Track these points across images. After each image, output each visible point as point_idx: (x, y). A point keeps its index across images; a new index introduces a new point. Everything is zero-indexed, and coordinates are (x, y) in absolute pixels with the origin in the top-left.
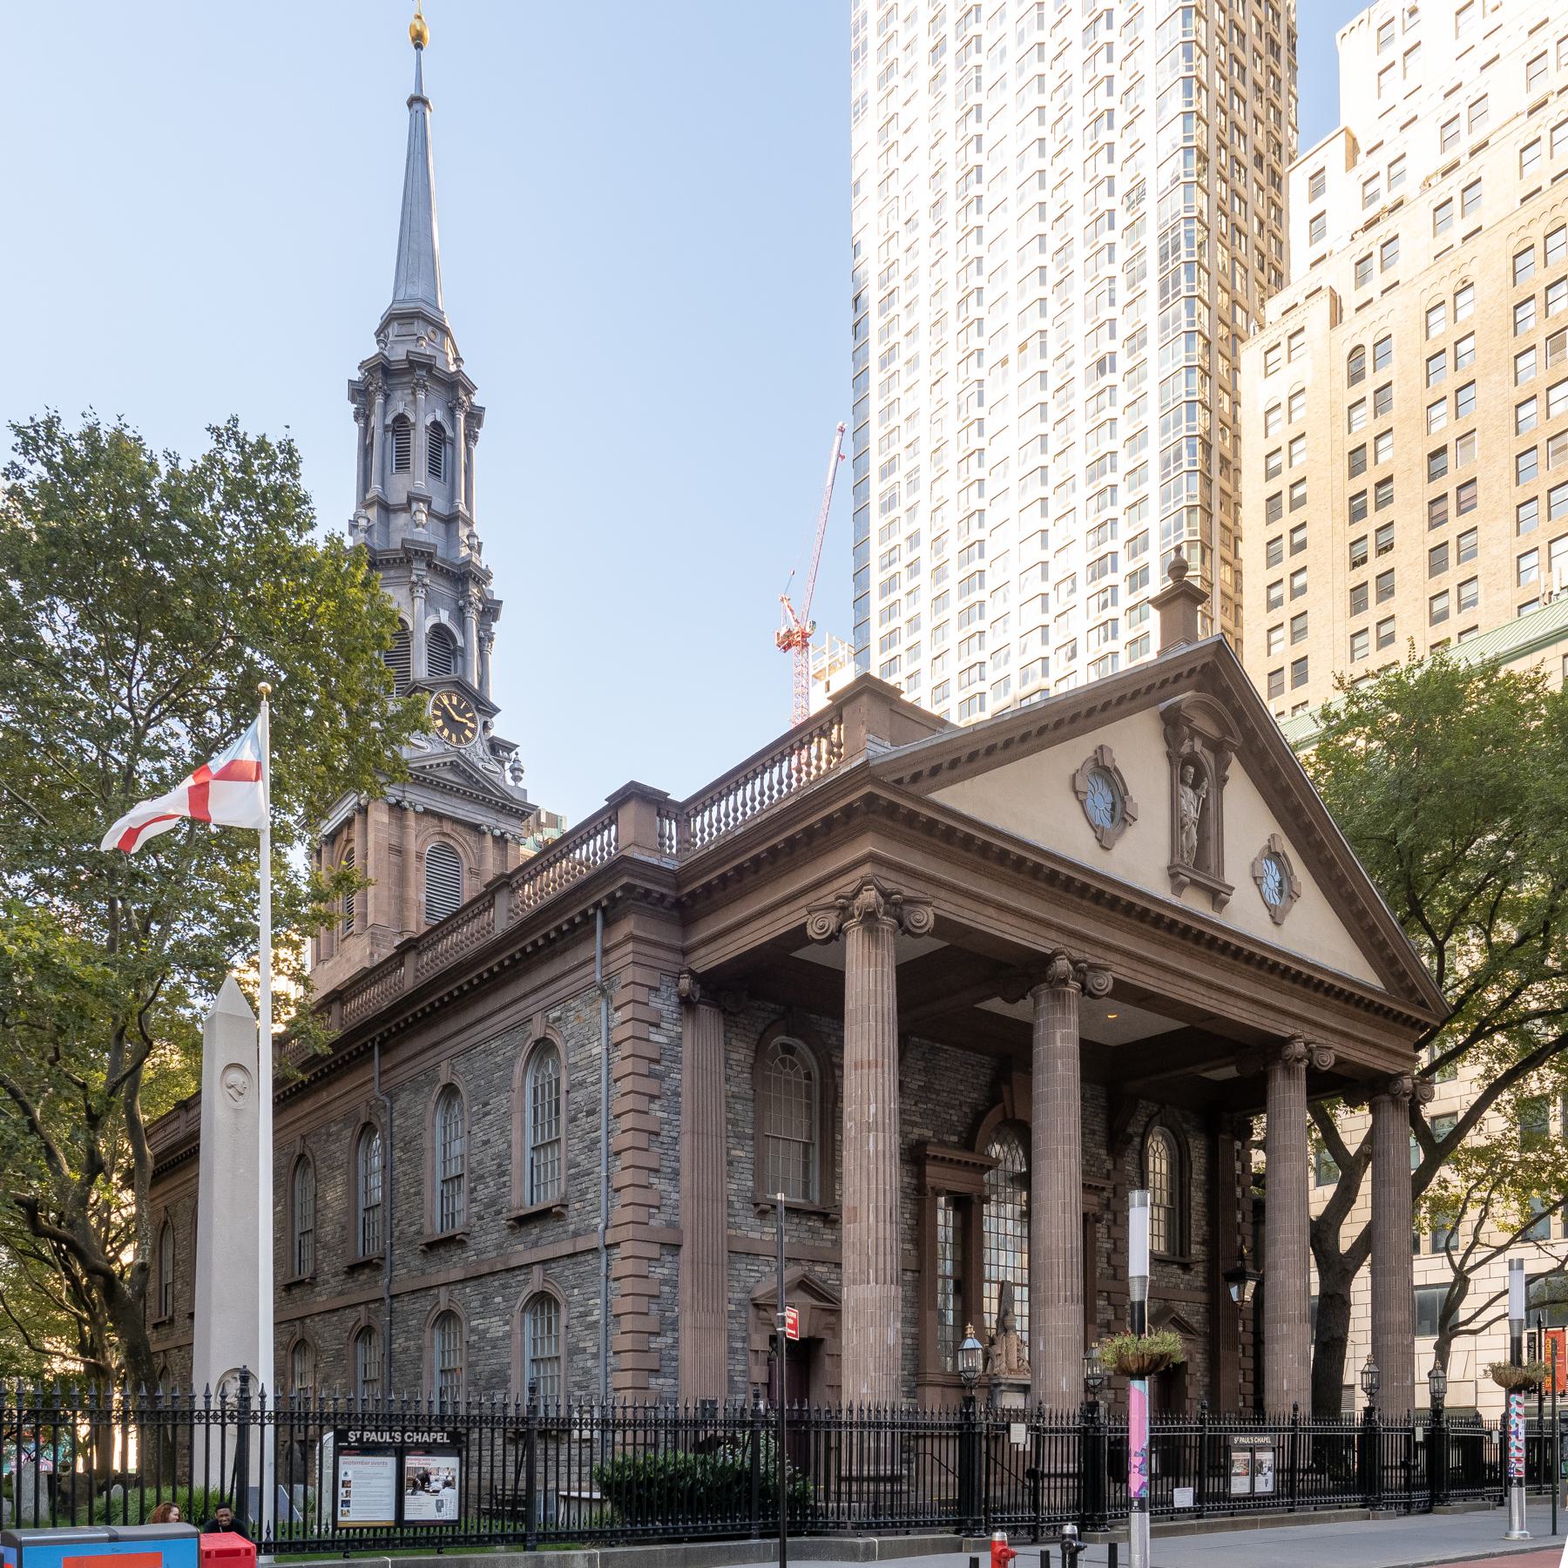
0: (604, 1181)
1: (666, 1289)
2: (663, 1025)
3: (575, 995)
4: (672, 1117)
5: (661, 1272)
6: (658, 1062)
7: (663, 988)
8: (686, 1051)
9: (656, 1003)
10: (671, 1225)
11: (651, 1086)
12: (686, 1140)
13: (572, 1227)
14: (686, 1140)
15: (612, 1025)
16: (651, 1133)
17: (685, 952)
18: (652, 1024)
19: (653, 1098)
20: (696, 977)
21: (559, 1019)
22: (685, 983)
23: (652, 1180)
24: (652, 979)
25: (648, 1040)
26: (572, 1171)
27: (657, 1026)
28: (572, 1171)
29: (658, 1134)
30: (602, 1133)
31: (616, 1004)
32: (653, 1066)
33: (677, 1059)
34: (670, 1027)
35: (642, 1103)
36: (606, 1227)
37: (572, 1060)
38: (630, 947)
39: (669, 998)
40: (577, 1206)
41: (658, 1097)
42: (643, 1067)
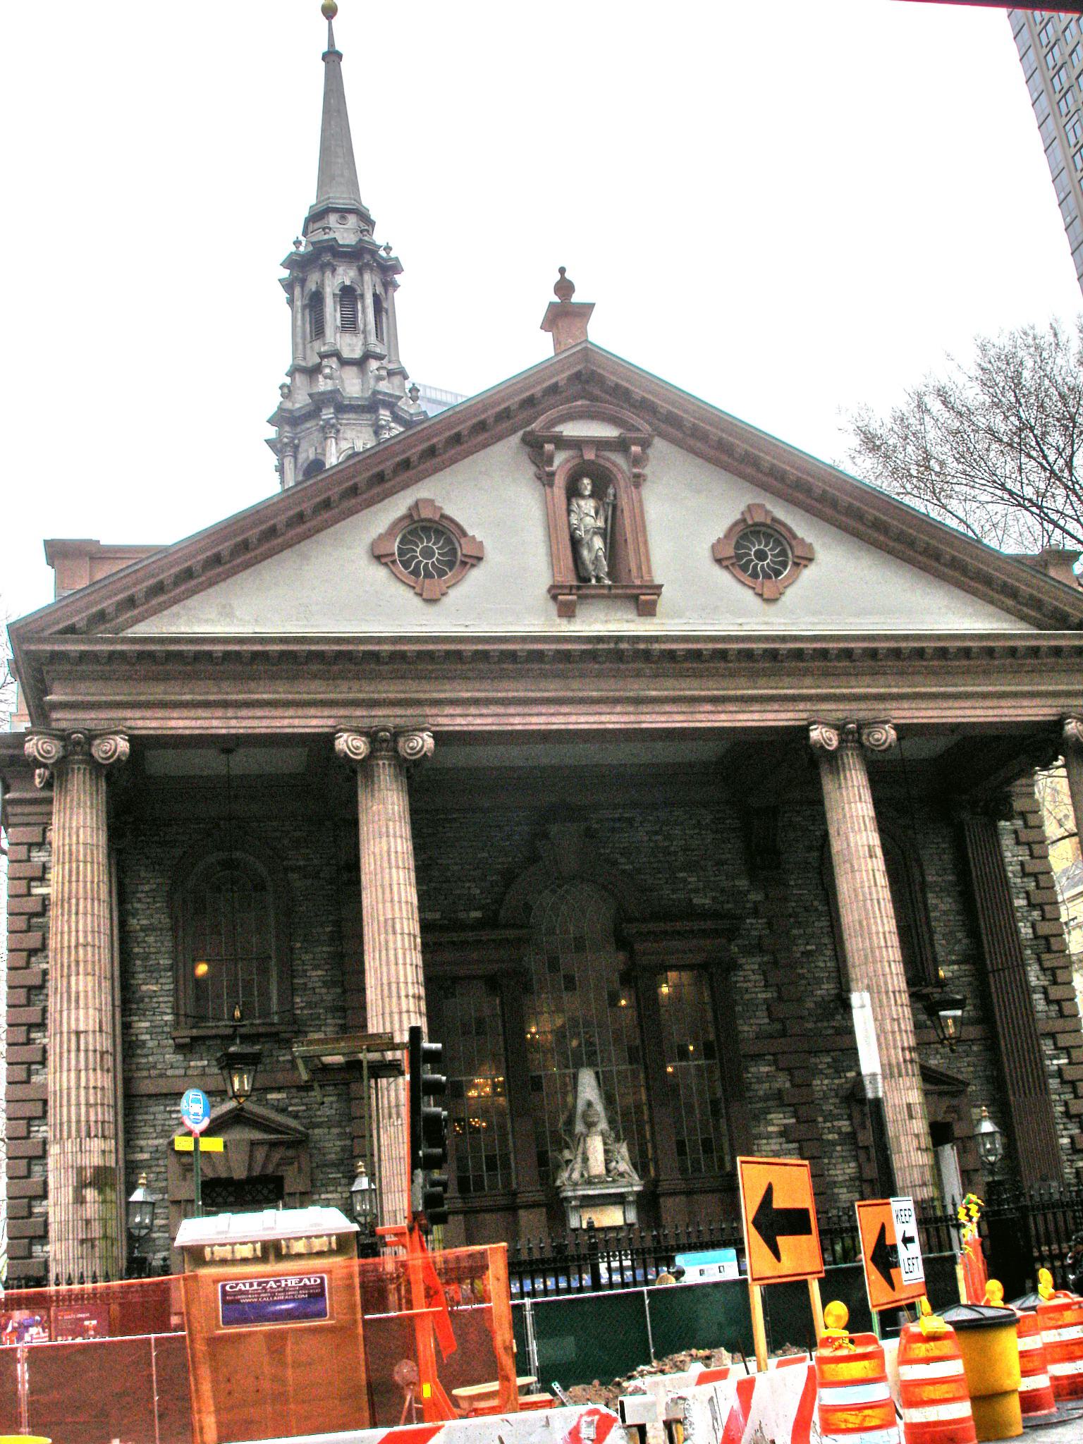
23: (33, 1035)
32: (35, 920)
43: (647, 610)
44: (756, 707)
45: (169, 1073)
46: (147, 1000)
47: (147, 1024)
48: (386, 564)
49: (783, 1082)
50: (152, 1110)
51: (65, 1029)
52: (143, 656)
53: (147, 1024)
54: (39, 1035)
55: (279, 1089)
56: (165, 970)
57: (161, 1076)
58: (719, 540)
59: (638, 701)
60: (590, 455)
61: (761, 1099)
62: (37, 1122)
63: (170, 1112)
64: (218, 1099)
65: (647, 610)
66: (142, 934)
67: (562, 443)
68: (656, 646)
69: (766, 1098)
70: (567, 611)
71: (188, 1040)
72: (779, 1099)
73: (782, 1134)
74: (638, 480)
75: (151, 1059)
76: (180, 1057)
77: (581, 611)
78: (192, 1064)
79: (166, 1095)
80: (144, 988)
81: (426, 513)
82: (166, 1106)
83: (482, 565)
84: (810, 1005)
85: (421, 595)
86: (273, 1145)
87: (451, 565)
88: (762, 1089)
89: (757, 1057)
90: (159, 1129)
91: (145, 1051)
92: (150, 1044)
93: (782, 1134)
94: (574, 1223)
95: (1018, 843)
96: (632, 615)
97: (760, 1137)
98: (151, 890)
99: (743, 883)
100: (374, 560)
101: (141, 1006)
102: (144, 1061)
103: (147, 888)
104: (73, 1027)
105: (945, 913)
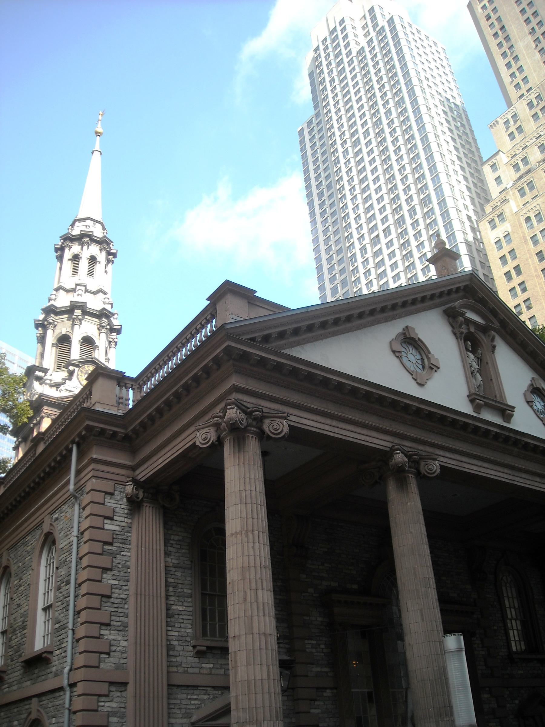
0: (70, 632)
1: (114, 719)
2: (115, 518)
3: (64, 503)
4: (122, 583)
5: (107, 706)
6: (111, 544)
7: (116, 493)
8: (133, 537)
9: (110, 503)
10: (119, 667)
11: (105, 561)
12: (132, 600)
13: (54, 669)
14: (132, 600)
15: (81, 520)
16: (103, 596)
17: (134, 468)
18: (106, 518)
19: (105, 570)
20: (137, 483)
21: (57, 519)
22: (129, 488)
23: (103, 632)
24: (108, 486)
25: (103, 529)
26: (57, 626)
27: (111, 519)
28: (57, 626)
29: (109, 597)
30: (72, 598)
31: (83, 505)
32: (106, 547)
33: (125, 542)
34: (122, 519)
35: (96, 574)
36: (71, 670)
37: (61, 546)
38: (92, 466)
39: (122, 499)
40: (58, 652)
41: (111, 570)
42: (98, 547)
45: (191, 670)
46: (176, 616)
47: (176, 634)
48: (398, 357)
50: (179, 696)
51: (256, 630)
52: (294, 372)
53: (176, 634)
54: (107, 632)
56: (188, 597)
57: (186, 672)
58: (525, 391)
62: (103, 699)
63: (190, 699)
64: (220, 692)
66: (174, 569)
70: (477, 409)
71: (205, 648)
75: (178, 659)
76: (197, 660)
78: (204, 665)
79: (188, 686)
80: (174, 607)
82: (188, 694)
83: (438, 371)
85: (416, 380)
90: (183, 711)
91: (175, 653)
92: (178, 648)
98: (179, 540)
100: (392, 353)
101: (173, 619)
102: (174, 660)
103: (177, 538)
104: (263, 630)
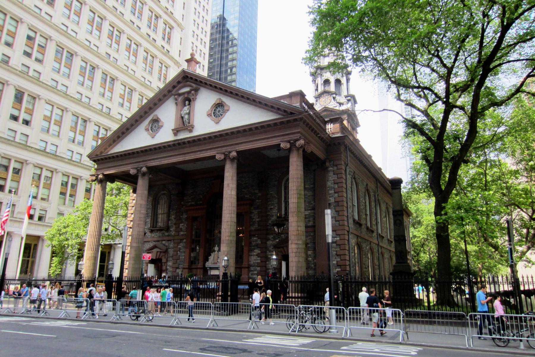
43: (191, 131)
44: (209, 151)
49: (259, 242)
55: (164, 241)
59: (184, 154)
60: (186, 96)
61: (254, 246)
65: (191, 131)
67: (180, 95)
68: (186, 140)
69: (254, 246)
72: (257, 246)
73: (257, 255)
74: (194, 100)
77: (179, 134)
81: (154, 118)
84: (270, 222)
86: (161, 252)
87: (158, 128)
88: (254, 243)
89: (254, 236)
93: (257, 255)
94: (209, 273)
95: (334, 174)
96: (188, 133)
97: (252, 255)
99: (257, 191)
105: (309, 196)
